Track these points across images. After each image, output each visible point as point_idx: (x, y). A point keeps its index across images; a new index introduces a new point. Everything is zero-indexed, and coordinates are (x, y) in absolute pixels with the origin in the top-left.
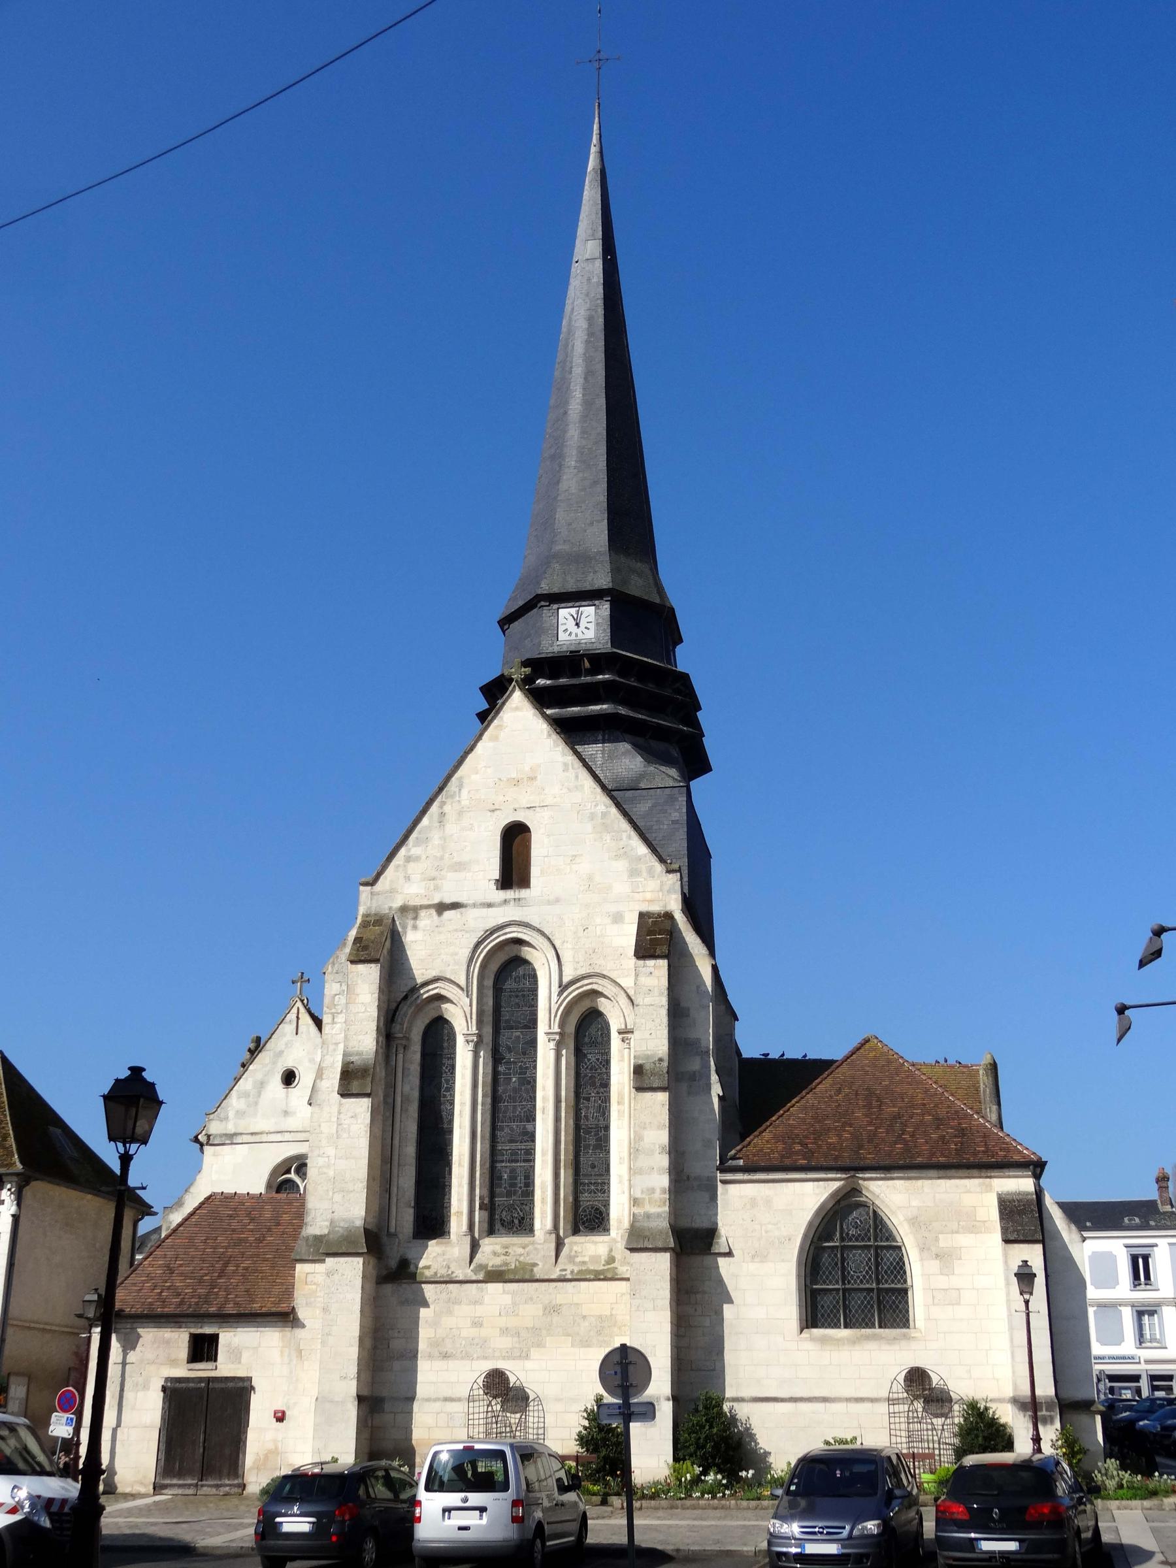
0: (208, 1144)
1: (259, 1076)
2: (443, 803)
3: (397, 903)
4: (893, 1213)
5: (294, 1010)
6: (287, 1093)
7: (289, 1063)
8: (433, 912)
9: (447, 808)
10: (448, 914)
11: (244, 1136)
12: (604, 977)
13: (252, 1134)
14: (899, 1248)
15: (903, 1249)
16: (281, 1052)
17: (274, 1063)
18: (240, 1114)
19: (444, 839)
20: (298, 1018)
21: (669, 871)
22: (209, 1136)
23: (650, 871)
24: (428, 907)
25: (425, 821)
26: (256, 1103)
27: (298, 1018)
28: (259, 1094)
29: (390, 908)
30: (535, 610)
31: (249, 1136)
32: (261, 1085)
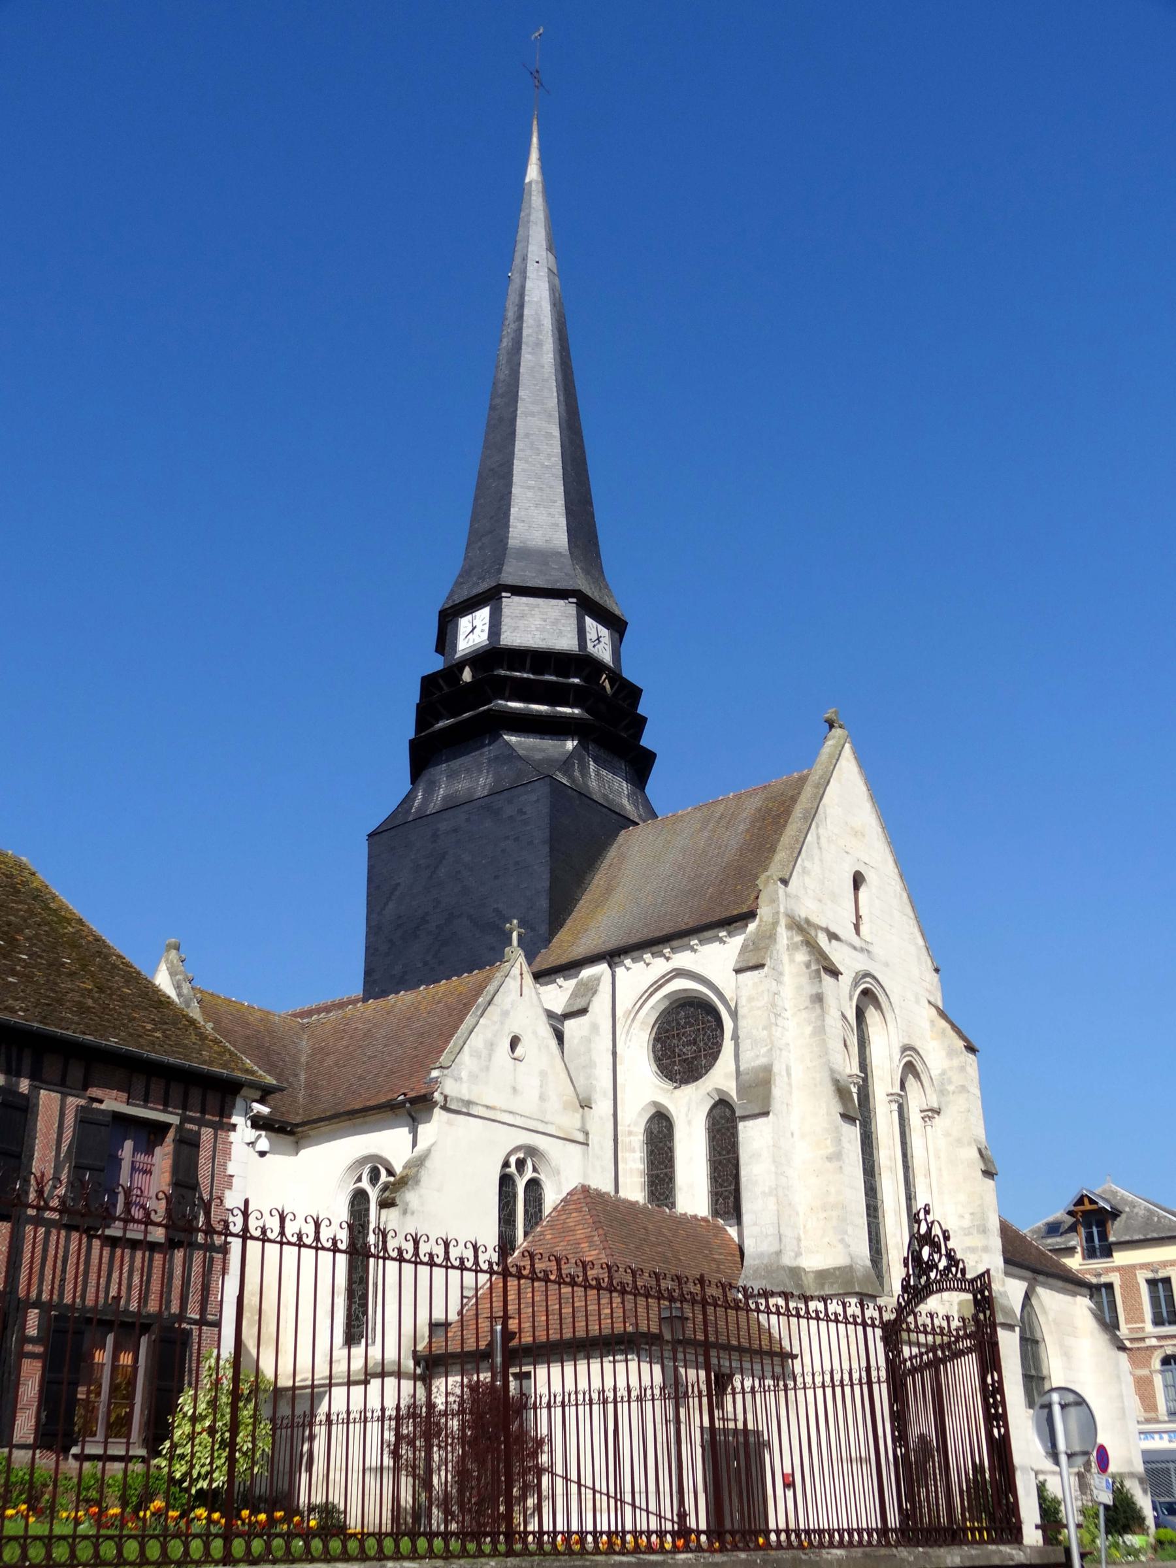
0: (445, 1108)
1: (490, 1035)
2: (817, 827)
3: (803, 915)
4: (1045, 1312)
5: (518, 965)
6: (515, 1065)
7: (517, 1031)
8: (826, 938)
9: (821, 831)
10: (834, 942)
11: (480, 1108)
12: (918, 1054)
13: (487, 1107)
14: (1037, 1342)
15: (1042, 1346)
16: (505, 1014)
17: (502, 1023)
18: (474, 1077)
19: (821, 860)
20: (521, 974)
21: (937, 970)
22: (446, 1097)
23: (926, 962)
24: (822, 929)
25: (809, 837)
26: (487, 1068)
27: (521, 974)
28: (490, 1056)
29: (799, 916)
30: (561, 602)
31: (484, 1109)
32: (491, 1046)
